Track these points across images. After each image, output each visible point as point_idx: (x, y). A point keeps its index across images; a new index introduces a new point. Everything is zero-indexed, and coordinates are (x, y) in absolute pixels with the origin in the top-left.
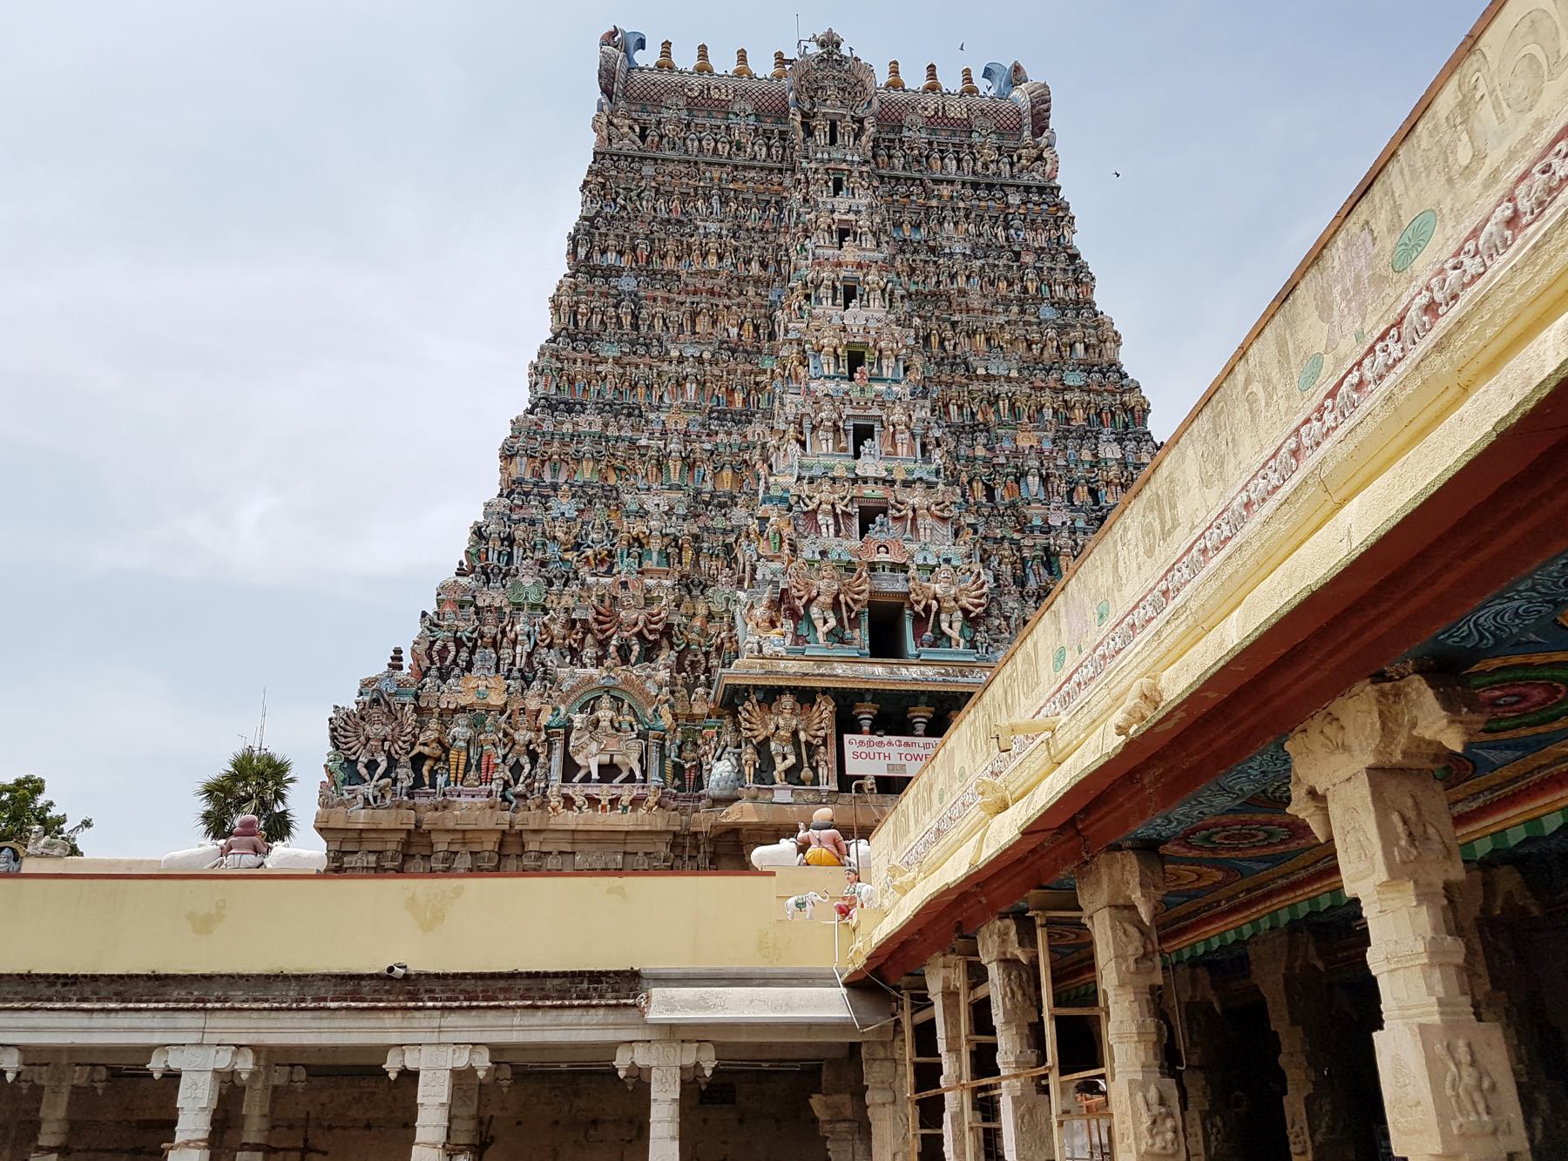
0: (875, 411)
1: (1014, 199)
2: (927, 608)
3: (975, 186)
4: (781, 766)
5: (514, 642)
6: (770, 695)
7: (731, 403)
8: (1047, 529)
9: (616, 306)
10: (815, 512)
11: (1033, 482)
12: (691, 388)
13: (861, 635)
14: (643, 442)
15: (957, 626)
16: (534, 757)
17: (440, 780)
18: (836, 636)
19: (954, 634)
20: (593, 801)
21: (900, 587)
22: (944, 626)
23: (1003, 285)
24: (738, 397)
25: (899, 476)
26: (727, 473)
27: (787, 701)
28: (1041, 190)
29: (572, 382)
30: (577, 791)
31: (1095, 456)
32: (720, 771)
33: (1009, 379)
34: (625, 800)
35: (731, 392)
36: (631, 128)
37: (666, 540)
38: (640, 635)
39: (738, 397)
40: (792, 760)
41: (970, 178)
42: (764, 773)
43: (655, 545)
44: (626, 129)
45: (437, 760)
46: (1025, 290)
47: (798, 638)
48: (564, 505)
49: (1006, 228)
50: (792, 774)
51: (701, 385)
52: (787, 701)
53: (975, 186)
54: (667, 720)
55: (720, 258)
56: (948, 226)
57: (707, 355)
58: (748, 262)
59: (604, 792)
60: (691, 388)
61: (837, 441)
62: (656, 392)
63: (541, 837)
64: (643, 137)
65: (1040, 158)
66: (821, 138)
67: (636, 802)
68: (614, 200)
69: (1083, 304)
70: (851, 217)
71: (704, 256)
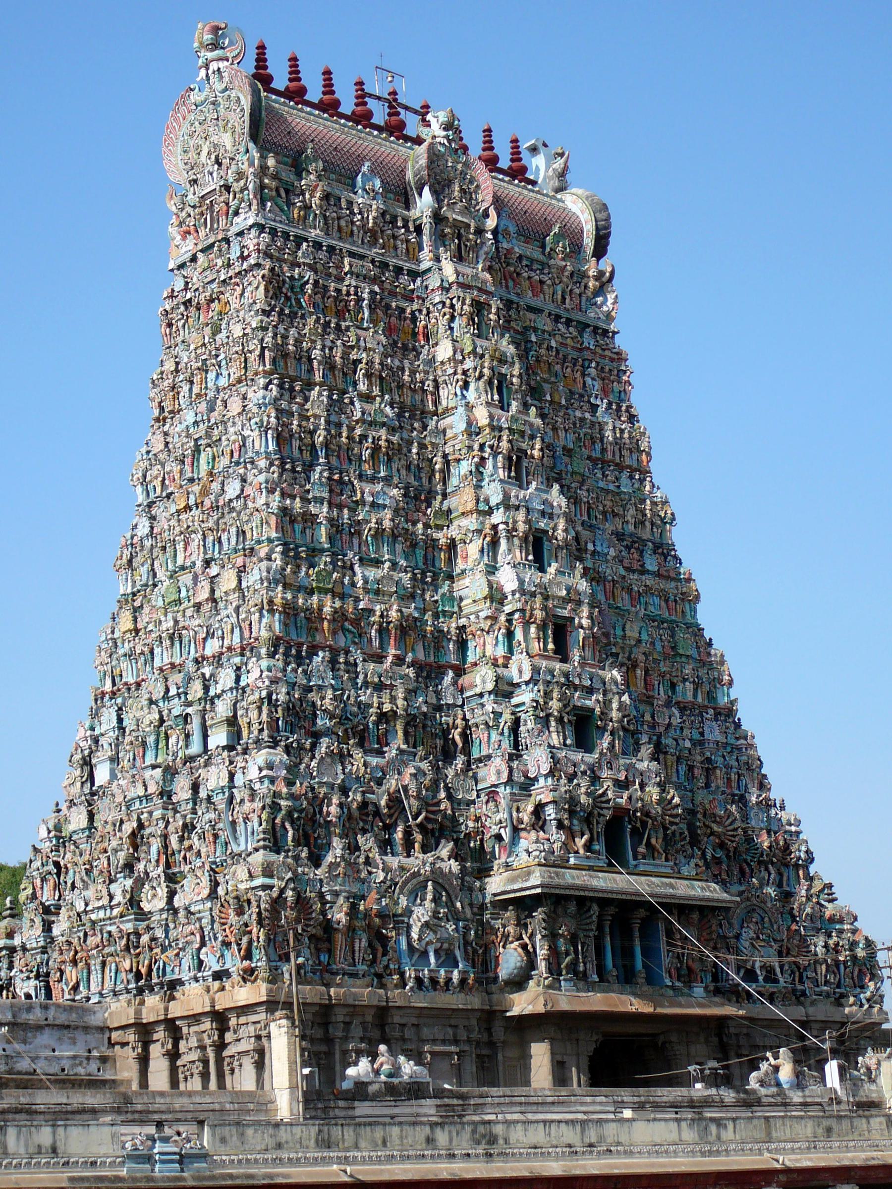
2: (644, 824)
15: (660, 841)
18: (588, 847)
19: (658, 846)
22: (653, 841)
27: (572, 908)
28: (606, 332)
32: (509, 960)
36: (277, 190)
37: (409, 719)
38: (420, 826)
44: (274, 193)
49: (583, 375)
53: (557, 318)
63: (402, 1012)
68: (280, 288)
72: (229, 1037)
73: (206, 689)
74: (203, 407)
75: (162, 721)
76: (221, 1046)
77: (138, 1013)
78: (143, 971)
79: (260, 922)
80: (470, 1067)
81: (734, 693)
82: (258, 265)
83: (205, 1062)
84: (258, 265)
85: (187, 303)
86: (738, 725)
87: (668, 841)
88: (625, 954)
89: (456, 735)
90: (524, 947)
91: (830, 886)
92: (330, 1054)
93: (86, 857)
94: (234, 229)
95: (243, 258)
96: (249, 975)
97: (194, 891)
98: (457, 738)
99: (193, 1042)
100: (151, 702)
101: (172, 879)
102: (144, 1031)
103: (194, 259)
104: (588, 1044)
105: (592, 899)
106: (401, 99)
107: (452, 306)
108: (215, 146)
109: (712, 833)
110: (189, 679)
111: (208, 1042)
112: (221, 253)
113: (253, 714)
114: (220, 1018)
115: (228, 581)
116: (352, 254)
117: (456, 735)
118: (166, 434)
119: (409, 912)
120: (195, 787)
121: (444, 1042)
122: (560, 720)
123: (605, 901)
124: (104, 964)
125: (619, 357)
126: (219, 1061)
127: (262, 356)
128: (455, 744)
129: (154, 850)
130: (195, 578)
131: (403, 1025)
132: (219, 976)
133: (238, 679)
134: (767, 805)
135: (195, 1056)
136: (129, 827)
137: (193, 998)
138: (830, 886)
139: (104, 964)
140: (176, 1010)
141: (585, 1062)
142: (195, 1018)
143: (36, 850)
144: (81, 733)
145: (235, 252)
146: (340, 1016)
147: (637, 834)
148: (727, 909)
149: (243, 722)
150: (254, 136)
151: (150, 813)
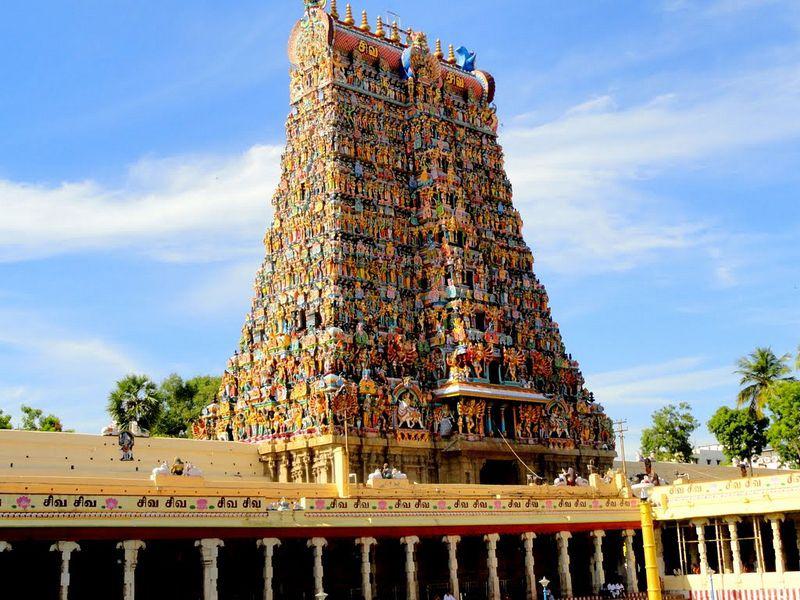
0: (474, 267)
1: (484, 141)
3: (470, 130)
4: (470, 427)
5: (361, 362)
6: (467, 399)
7: (402, 240)
8: (512, 319)
9: (356, 182)
10: (463, 315)
11: (506, 295)
12: (390, 232)
13: (487, 374)
14: (381, 261)
16: (386, 416)
17: (359, 423)
18: (482, 375)
20: (410, 437)
21: (497, 355)
23: (483, 188)
24: (405, 238)
25: (486, 300)
26: (408, 280)
27: (473, 402)
29: (346, 223)
30: (406, 432)
31: (522, 284)
33: (492, 241)
34: (419, 435)
35: (402, 235)
38: (404, 364)
39: (405, 238)
40: (473, 424)
41: (466, 124)
42: (465, 430)
43: (395, 318)
45: (356, 415)
46: (491, 192)
47: (470, 375)
48: (359, 292)
50: (473, 430)
51: (393, 231)
52: (473, 402)
54: (425, 404)
55: (388, 157)
56: (463, 152)
57: (393, 214)
58: (396, 161)
59: (413, 433)
60: (390, 232)
61: (463, 280)
62: (376, 232)
64: (346, 75)
65: (490, 118)
66: (420, 97)
67: (423, 436)
69: (508, 204)
70: (446, 154)
71: (383, 155)
72: (315, 460)
73: (306, 299)
74: (305, 169)
75: (285, 314)
76: (311, 463)
77: (273, 448)
78: (276, 429)
79: (330, 407)
80: (425, 474)
81: (548, 305)
82: (332, 103)
83: (304, 471)
84: (332, 103)
85: (298, 121)
86: (550, 320)
87: (518, 372)
88: (497, 425)
89: (421, 322)
90: (451, 420)
91: (591, 394)
92: (362, 467)
93: (249, 376)
94: (321, 86)
95: (325, 100)
96: (325, 431)
97: (299, 392)
98: (422, 325)
99: (298, 461)
100: (280, 305)
101: (289, 387)
102: (276, 456)
103: (301, 100)
104: (480, 463)
105: (482, 398)
106: (400, 27)
107: (422, 124)
108: (313, 47)
109: (538, 369)
110: (297, 294)
111: (305, 461)
112: (314, 98)
113: (327, 311)
114: (311, 452)
115: (316, 250)
116: (375, 98)
117: (421, 322)
118: (288, 181)
119: (398, 404)
120: (300, 346)
121: (413, 463)
122: (469, 316)
123: (488, 400)
124: (258, 425)
125: (499, 149)
126: (311, 470)
127: (333, 145)
128: (420, 327)
129: (281, 372)
130: (301, 248)
131: (395, 455)
132: (310, 431)
133: (320, 296)
134: (564, 356)
135: (299, 468)
136: (270, 362)
137: (298, 442)
138: (591, 394)
139: (258, 425)
140: (290, 447)
141: (478, 473)
142: (299, 451)
143: (226, 373)
144: (247, 319)
145: (321, 97)
146: (366, 450)
147: (504, 370)
148: (544, 404)
149: (322, 315)
150: (330, 44)
151: (279, 356)
